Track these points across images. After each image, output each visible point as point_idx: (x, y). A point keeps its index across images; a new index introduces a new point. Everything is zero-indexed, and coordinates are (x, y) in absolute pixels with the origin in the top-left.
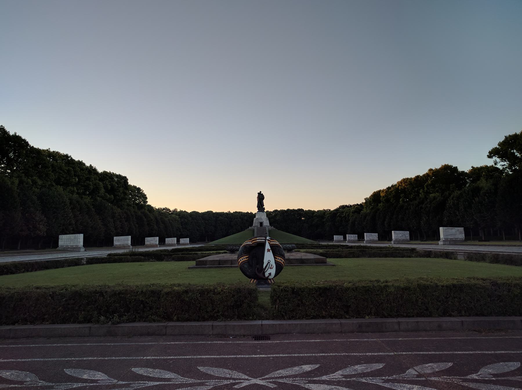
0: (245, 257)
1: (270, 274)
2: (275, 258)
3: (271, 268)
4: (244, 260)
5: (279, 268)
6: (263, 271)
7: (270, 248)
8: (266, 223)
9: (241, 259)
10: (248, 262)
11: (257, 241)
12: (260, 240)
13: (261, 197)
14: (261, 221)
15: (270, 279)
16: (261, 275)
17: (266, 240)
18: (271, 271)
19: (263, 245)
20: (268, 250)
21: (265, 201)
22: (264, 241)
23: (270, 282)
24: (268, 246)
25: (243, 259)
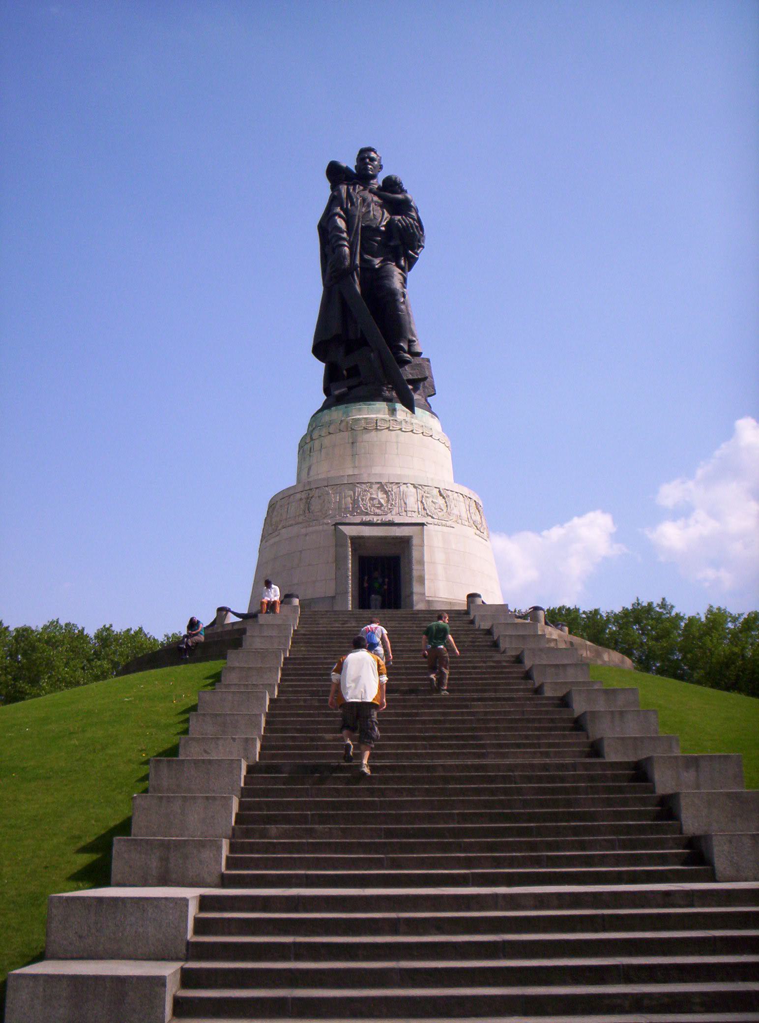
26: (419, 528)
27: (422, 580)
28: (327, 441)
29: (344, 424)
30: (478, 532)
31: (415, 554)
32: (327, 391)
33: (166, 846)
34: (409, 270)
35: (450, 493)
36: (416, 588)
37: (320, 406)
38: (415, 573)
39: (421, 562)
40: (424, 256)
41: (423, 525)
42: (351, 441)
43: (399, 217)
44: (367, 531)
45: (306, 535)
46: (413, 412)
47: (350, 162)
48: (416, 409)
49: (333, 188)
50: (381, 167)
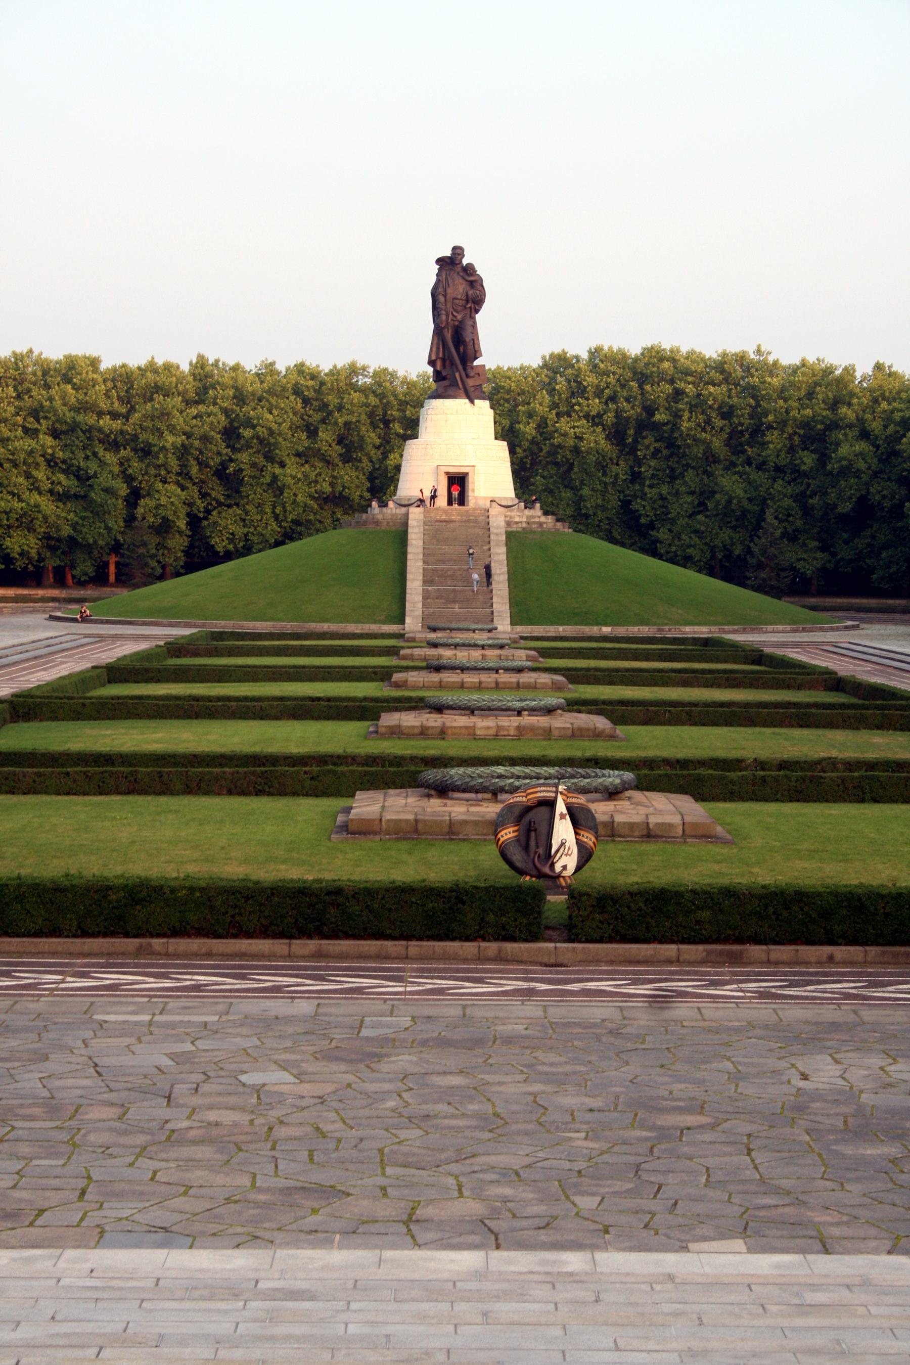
0: (511, 830)
1: (565, 867)
2: (576, 833)
3: (566, 855)
4: (509, 836)
5: (585, 855)
6: (548, 857)
7: (565, 811)
8: (493, 477)
9: (503, 833)
10: (517, 840)
11: (539, 795)
12: (544, 793)
13: (457, 291)
14: (457, 465)
15: (564, 877)
16: (546, 870)
17: (556, 792)
18: (567, 862)
19: (550, 804)
20: (562, 816)
21: (486, 322)
22: (553, 795)
23: (564, 884)
24: (561, 808)
25: (508, 834)
27: (473, 491)
39: (473, 483)
47: (448, 253)
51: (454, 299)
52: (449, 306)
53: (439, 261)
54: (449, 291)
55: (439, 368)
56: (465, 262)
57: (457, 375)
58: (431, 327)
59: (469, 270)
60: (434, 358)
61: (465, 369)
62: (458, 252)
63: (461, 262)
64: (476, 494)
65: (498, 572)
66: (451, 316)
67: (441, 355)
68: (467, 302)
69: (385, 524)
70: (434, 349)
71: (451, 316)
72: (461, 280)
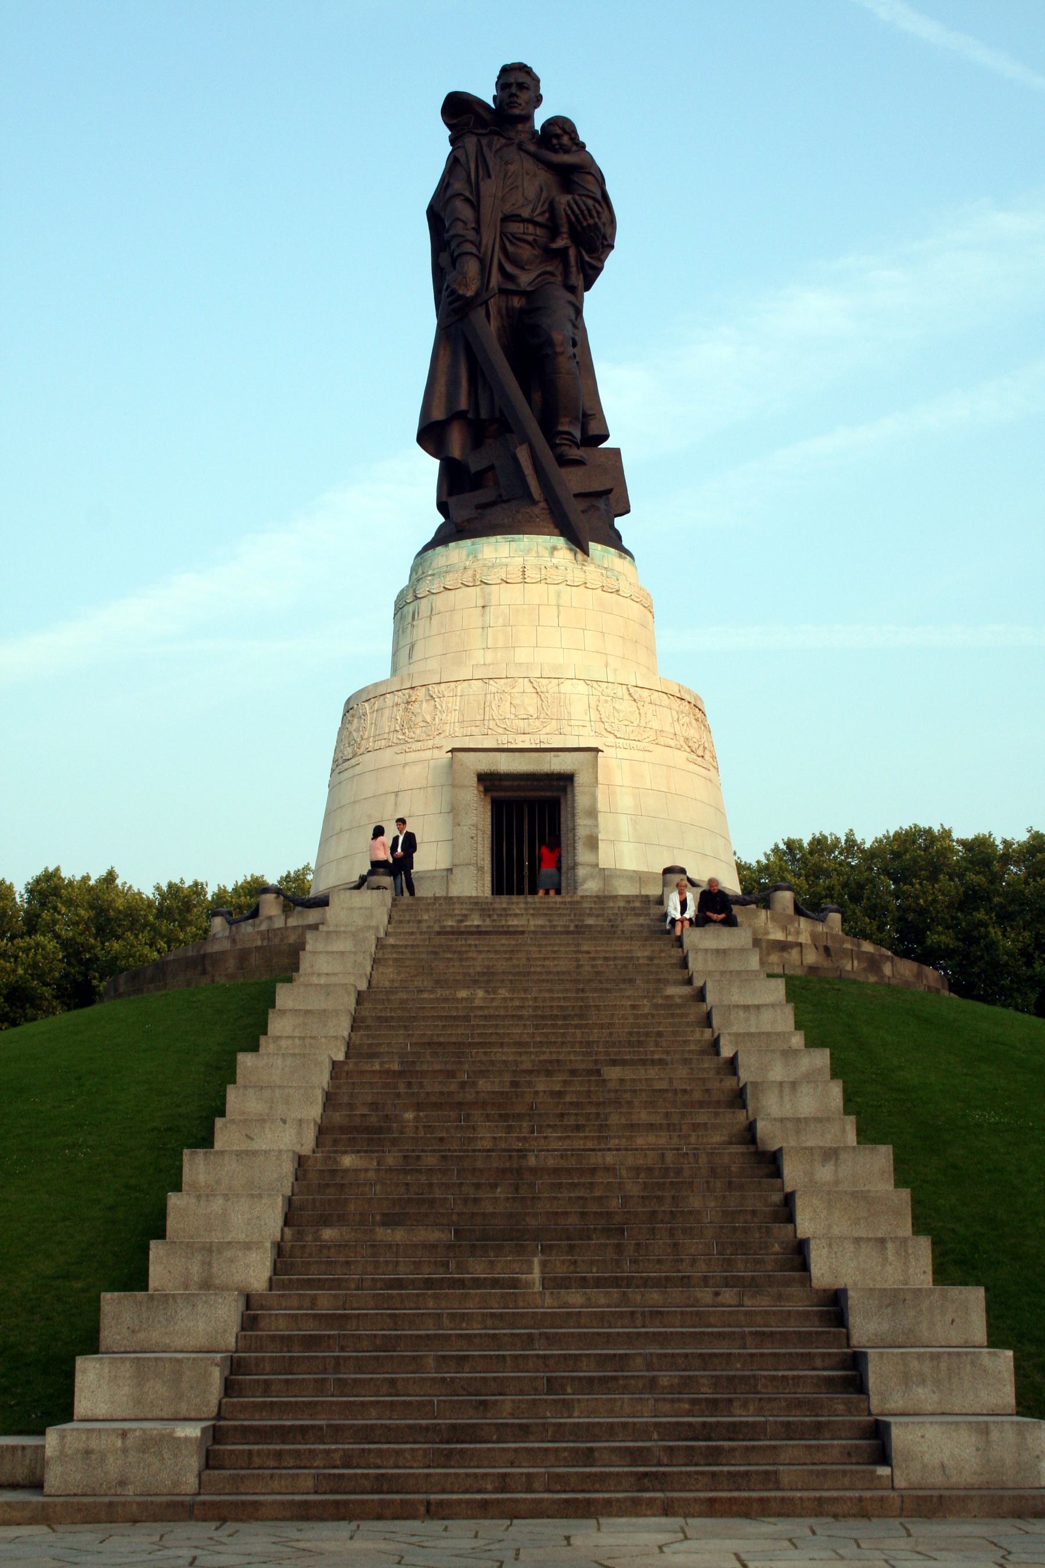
26: (593, 754)
27: (593, 843)
28: (441, 602)
29: (470, 572)
30: (693, 756)
31: (581, 801)
32: (442, 507)
33: (209, 1249)
34: (588, 287)
35: (646, 693)
36: (583, 855)
37: (429, 536)
38: (582, 832)
39: (593, 813)
40: (611, 262)
41: (597, 750)
42: (480, 603)
43: (569, 197)
44: (505, 764)
45: (405, 765)
46: (586, 552)
47: (486, 92)
48: (593, 546)
49: (452, 141)
50: (539, 99)
51: (506, 219)
52: (489, 237)
53: (458, 109)
54: (489, 188)
55: (456, 451)
56: (540, 117)
57: (523, 455)
58: (434, 322)
59: (561, 131)
60: (438, 415)
61: (550, 431)
62: (518, 82)
63: (529, 118)
64: (607, 857)
65: (777, 1072)
66: (495, 279)
67: (463, 404)
68: (553, 230)
69: (231, 964)
70: (441, 388)
71: (495, 279)
72: (529, 164)
